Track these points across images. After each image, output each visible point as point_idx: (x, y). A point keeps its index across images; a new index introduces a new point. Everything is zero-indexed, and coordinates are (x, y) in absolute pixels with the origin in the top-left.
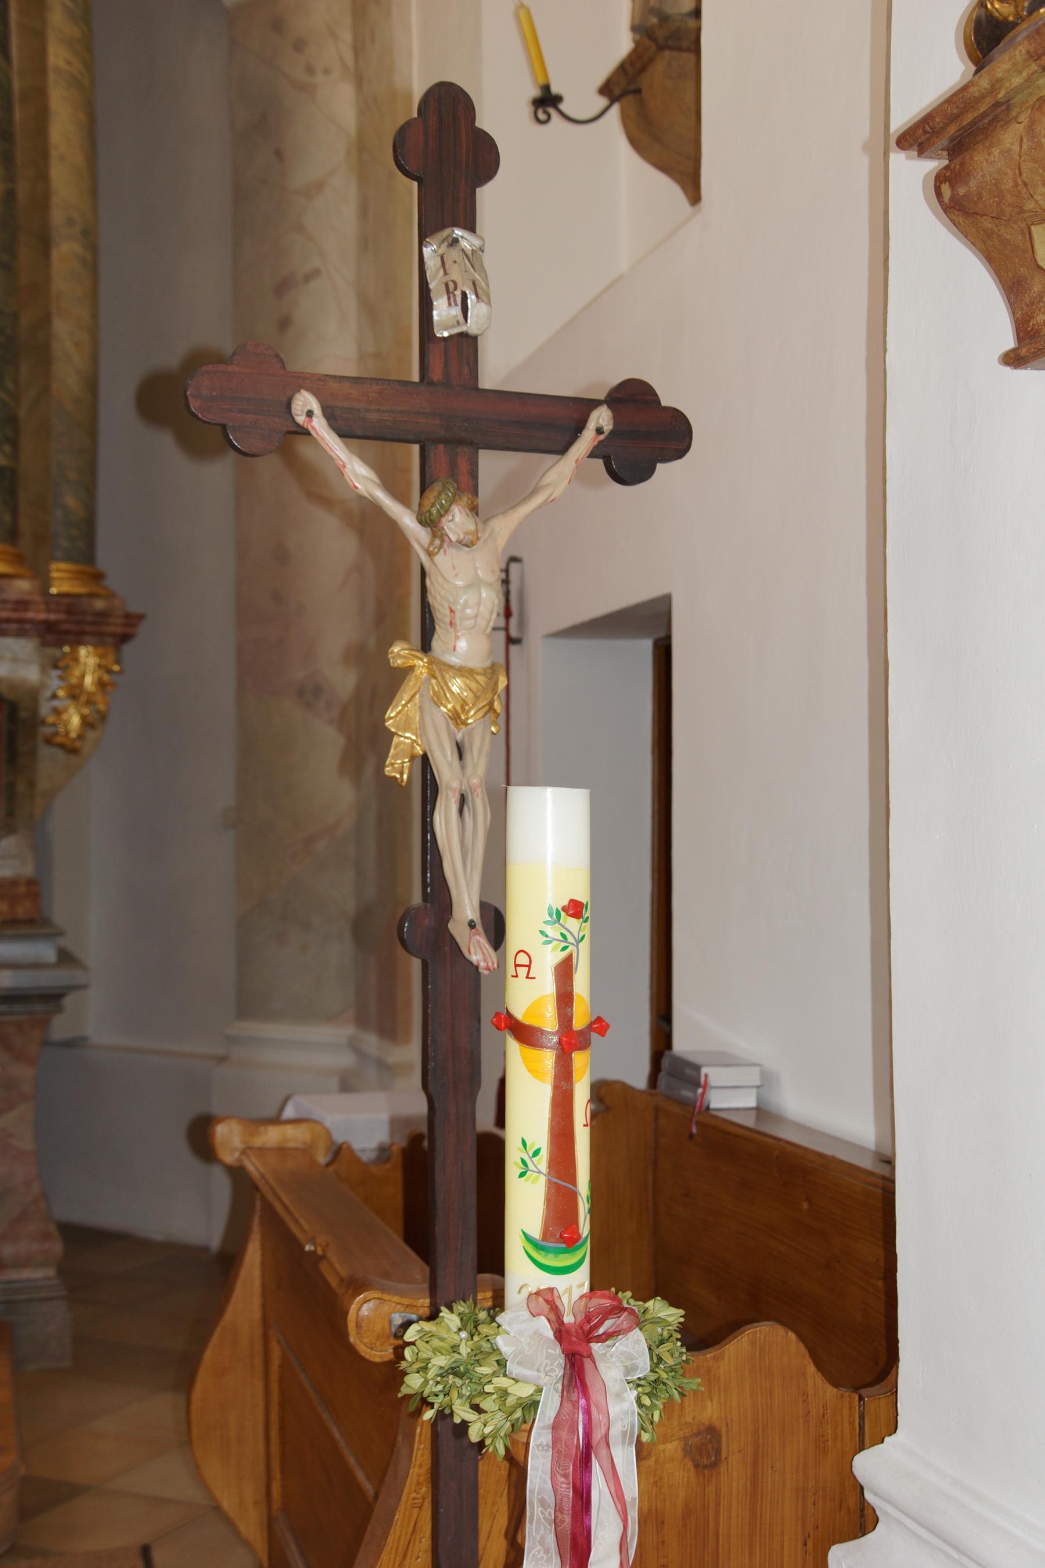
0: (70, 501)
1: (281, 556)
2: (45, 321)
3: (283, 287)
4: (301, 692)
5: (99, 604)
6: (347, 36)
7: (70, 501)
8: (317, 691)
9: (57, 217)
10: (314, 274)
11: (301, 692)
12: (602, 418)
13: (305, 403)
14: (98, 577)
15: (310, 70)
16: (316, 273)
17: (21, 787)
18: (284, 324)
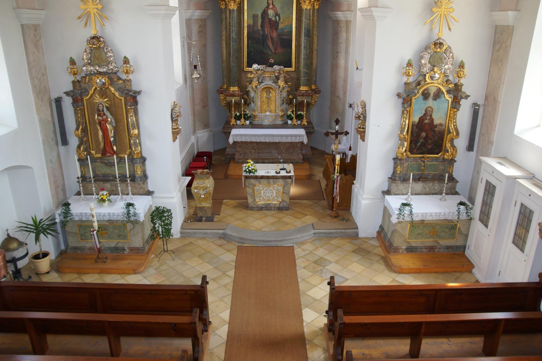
0: (314, 79)
1: (336, 82)
2: (313, 61)
3: (337, 52)
4: (337, 97)
5: (317, 90)
6: (345, 28)
7: (314, 79)
8: (339, 97)
9: (314, 49)
10: (340, 52)
11: (337, 97)
12: (344, 133)
13: (330, 134)
14: (316, 86)
15: (341, 30)
16: (341, 52)
17: (309, 109)
18: (337, 56)
